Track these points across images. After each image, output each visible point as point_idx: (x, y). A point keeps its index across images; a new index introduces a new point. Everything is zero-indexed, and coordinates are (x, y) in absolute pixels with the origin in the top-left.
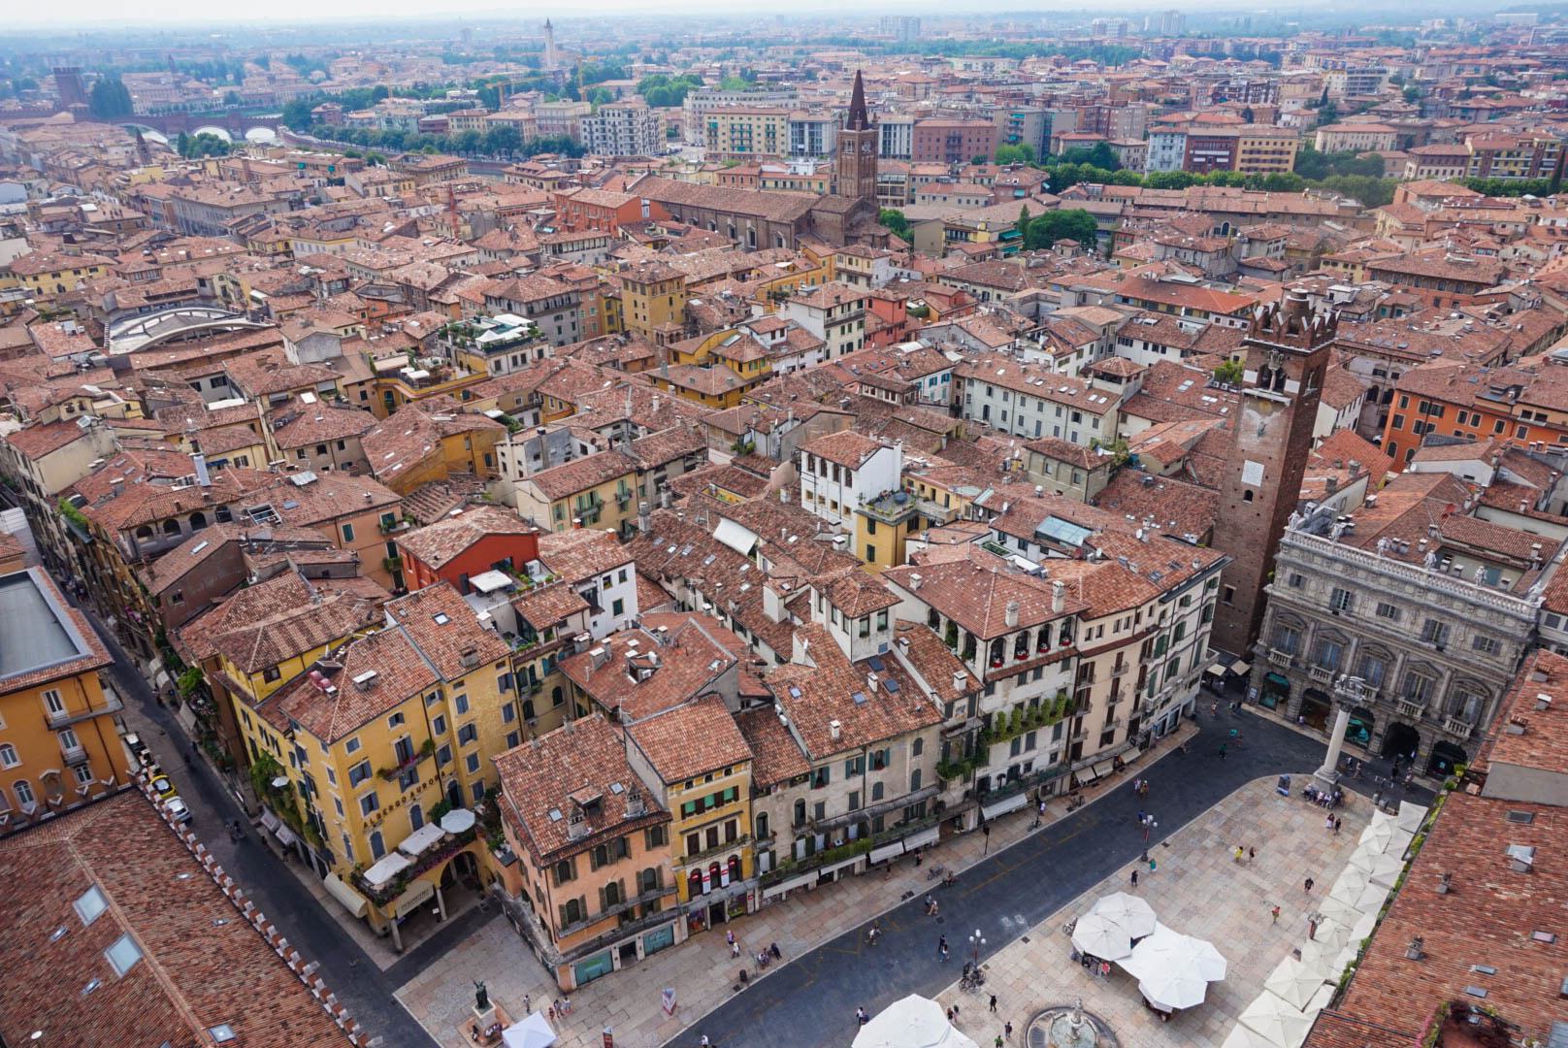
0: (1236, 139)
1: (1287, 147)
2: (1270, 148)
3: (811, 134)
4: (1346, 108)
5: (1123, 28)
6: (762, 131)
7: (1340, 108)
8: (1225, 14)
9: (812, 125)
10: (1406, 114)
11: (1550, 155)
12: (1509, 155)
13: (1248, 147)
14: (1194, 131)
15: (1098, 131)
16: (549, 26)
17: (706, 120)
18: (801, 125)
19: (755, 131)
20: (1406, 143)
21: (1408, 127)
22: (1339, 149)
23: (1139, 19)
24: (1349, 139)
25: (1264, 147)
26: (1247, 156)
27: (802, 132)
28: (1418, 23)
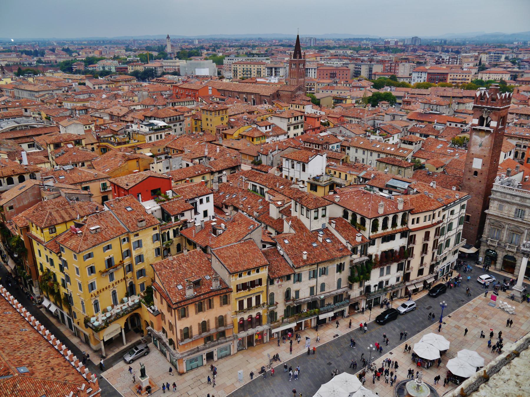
3: (275, 72)
4: (489, 66)
5: (396, 43)
6: (256, 71)
7: (486, 66)
8: (436, 40)
9: (276, 68)
10: (514, 68)
15: (390, 72)
16: (168, 37)
17: (233, 66)
18: (271, 68)
19: (253, 71)
20: (514, 78)
21: (514, 72)
22: (487, 79)
23: (403, 41)
24: (491, 75)
25: (458, 77)
27: (272, 71)
28: (512, 43)
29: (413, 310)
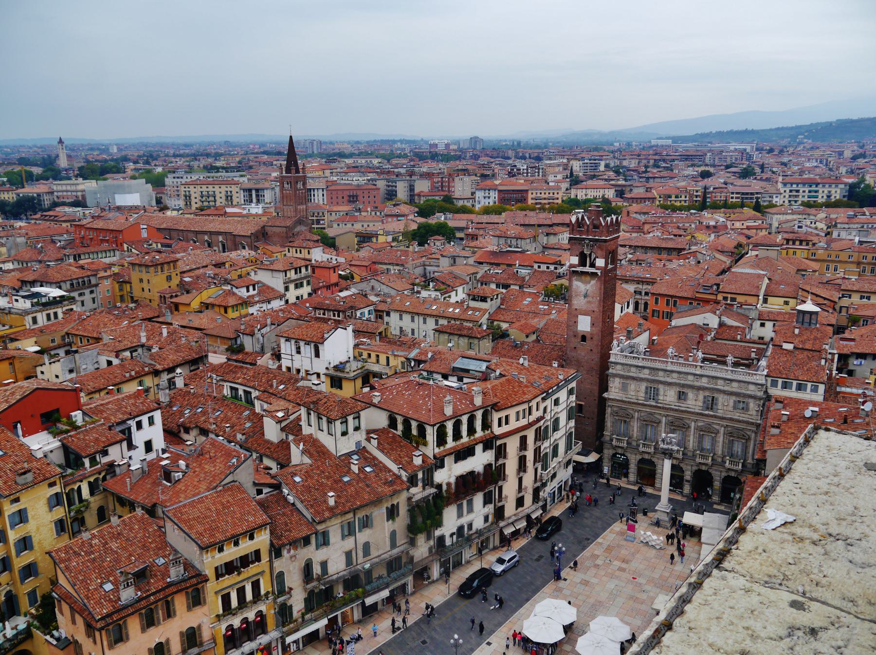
0: (527, 191)
1: (556, 195)
2: (547, 196)
3: (257, 196)
4: (584, 178)
5: (447, 146)
6: (223, 195)
7: (580, 178)
8: (506, 141)
9: (257, 190)
10: (618, 180)
11: (697, 196)
12: (677, 197)
13: (534, 195)
14: (501, 188)
15: (442, 190)
16: (61, 141)
17: (182, 189)
18: (250, 190)
20: (620, 194)
22: (584, 197)
23: (457, 143)
24: (589, 191)
25: (543, 196)
26: (534, 201)
27: (251, 195)
28: (612, 145)
29: (514, 566)
